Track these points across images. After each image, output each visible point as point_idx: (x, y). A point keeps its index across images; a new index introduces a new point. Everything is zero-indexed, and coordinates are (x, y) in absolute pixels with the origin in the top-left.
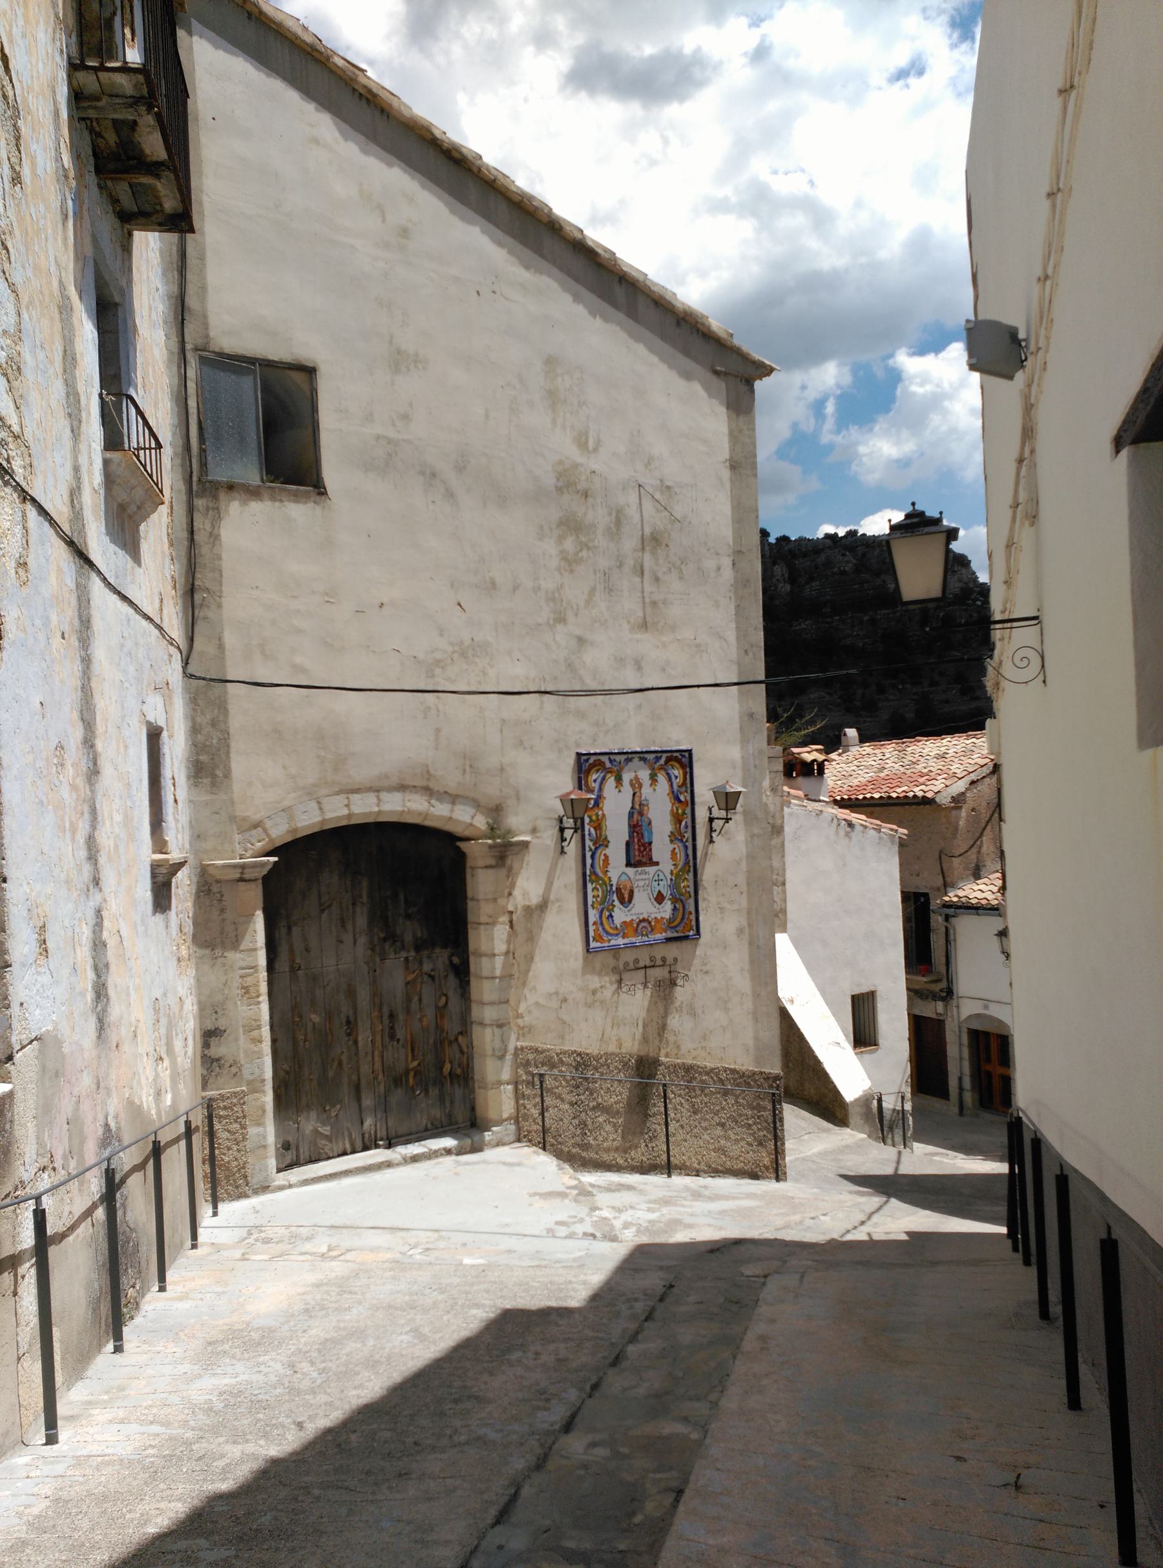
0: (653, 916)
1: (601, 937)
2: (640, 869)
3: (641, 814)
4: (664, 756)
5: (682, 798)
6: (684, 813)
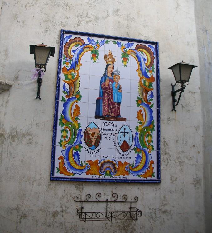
0: (117, 160)
1: (66, 170)
2: (108, 122)
3: (112, 80)
4: (135, 44)
5: (149, 75)
6: (150, 85)
